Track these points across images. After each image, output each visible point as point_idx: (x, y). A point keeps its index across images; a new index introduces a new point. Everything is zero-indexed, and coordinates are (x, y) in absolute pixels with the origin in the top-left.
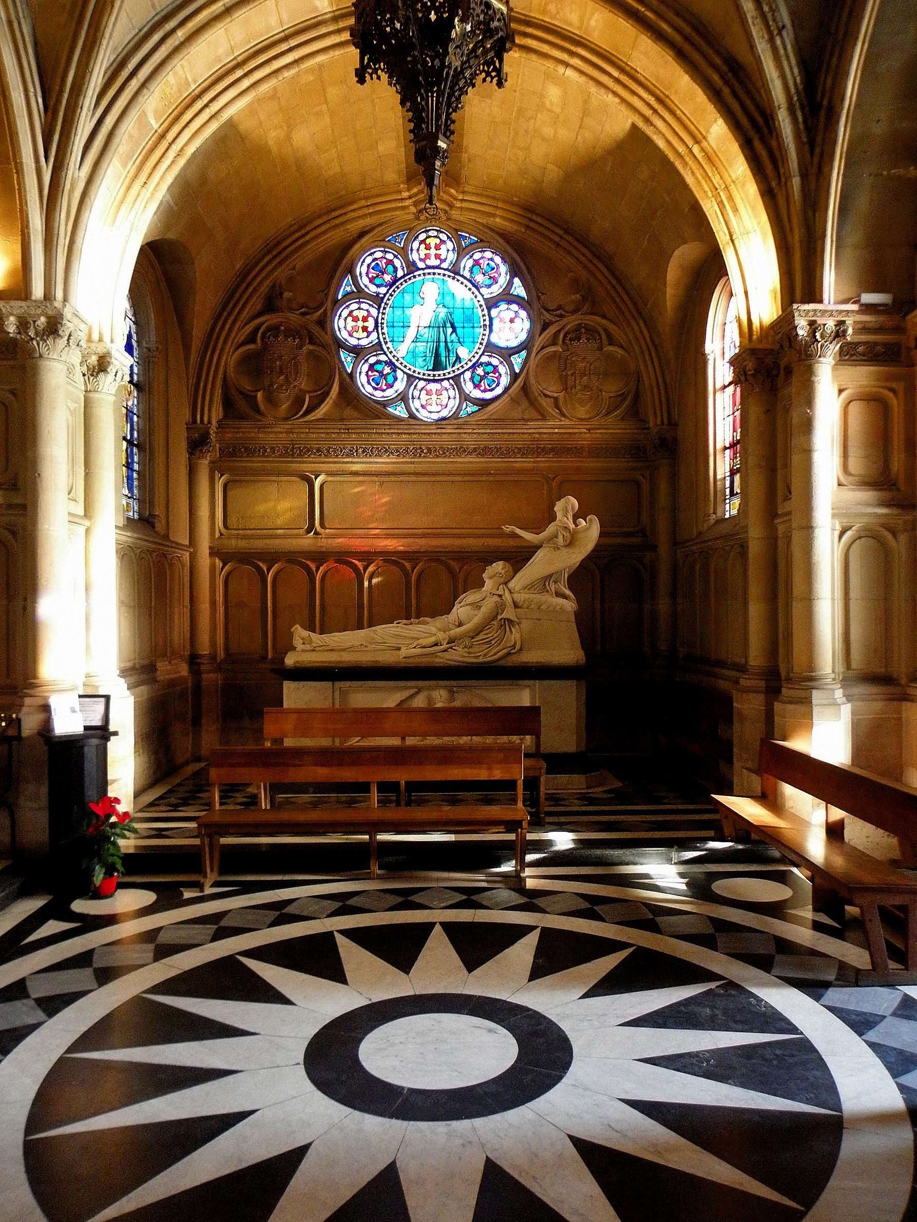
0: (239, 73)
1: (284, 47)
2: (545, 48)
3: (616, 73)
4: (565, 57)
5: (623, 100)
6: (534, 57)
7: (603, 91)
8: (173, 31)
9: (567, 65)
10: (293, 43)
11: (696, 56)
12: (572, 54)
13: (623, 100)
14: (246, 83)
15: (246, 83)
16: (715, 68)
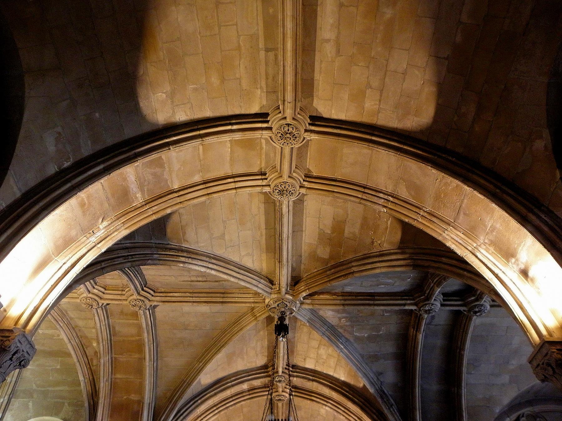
0: (215, 408)
1: (231, 399)
2: (318, 400)
3: (343, 409)
4: (325, 403)
5: (346, 418)
6: (315, 403)
7: (339, 415)
8: (197, 401)
9: (326, 406)
10: (234, 398)
11: (367, 409)
12: (327, 402)
13: (346, 418)
14: (217, 411)
15: (217, 411)
16: (375, 414)
